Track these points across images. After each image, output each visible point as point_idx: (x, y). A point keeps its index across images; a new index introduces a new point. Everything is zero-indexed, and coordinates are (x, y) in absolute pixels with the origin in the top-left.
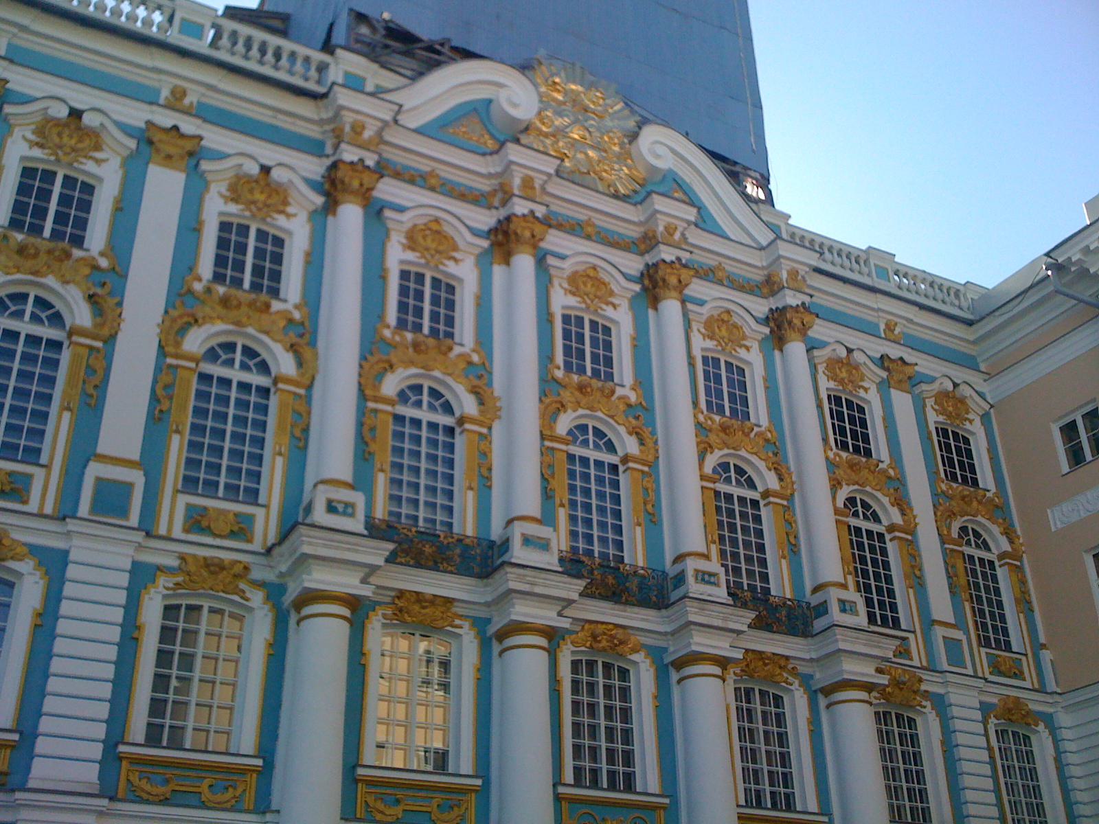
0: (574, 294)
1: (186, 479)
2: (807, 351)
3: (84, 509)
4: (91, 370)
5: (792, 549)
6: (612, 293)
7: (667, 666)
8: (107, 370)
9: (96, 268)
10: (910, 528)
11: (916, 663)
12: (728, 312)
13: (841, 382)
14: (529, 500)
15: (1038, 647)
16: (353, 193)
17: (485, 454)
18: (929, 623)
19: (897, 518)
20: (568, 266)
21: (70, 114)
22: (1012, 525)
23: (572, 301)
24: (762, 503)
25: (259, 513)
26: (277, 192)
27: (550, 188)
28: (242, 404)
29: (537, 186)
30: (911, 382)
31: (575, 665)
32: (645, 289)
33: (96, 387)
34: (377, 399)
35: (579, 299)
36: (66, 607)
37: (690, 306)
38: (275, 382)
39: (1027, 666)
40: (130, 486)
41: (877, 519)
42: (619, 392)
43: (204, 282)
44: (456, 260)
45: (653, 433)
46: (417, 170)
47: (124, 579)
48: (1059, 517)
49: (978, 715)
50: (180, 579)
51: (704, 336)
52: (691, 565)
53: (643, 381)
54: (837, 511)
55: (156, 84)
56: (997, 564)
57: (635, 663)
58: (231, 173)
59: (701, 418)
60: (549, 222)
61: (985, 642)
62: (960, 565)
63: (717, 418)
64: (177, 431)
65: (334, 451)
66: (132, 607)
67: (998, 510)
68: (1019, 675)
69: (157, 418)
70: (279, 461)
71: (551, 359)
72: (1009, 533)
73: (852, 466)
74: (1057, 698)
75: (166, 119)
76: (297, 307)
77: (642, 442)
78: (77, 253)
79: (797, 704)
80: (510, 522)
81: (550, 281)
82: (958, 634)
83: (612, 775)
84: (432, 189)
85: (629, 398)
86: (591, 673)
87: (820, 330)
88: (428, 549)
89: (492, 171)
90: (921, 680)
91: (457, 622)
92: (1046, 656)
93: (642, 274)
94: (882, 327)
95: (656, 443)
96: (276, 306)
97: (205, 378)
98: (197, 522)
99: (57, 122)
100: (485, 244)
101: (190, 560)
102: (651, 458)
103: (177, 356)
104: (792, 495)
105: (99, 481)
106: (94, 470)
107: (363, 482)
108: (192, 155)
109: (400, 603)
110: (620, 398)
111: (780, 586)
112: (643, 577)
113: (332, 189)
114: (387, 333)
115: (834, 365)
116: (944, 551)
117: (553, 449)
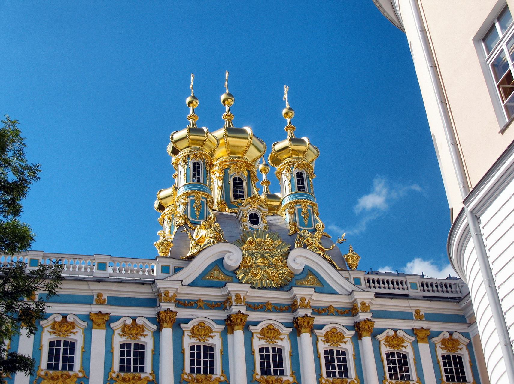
0: (263, 339)
9: (78, 378)
12: (334, 328)
20: (259, 327)
27: (248, 294)
29: (242, 297)
35: (265, 340)
37: (316, 331)
44: (212, 337)
51: (324, 342)
55: (91, 294)
71: (254, 371)
75: (96, 309)
76: (151, 374)
78: (71, 373)
81: (252, 336)
85: (289, 381)
89: (224, 293)
93: (293, 322)
94: (414, 313)
96: (143, 375)
100: (223, 327)
108: (108, 321)
113: (159, 321)
114: (186, 377)
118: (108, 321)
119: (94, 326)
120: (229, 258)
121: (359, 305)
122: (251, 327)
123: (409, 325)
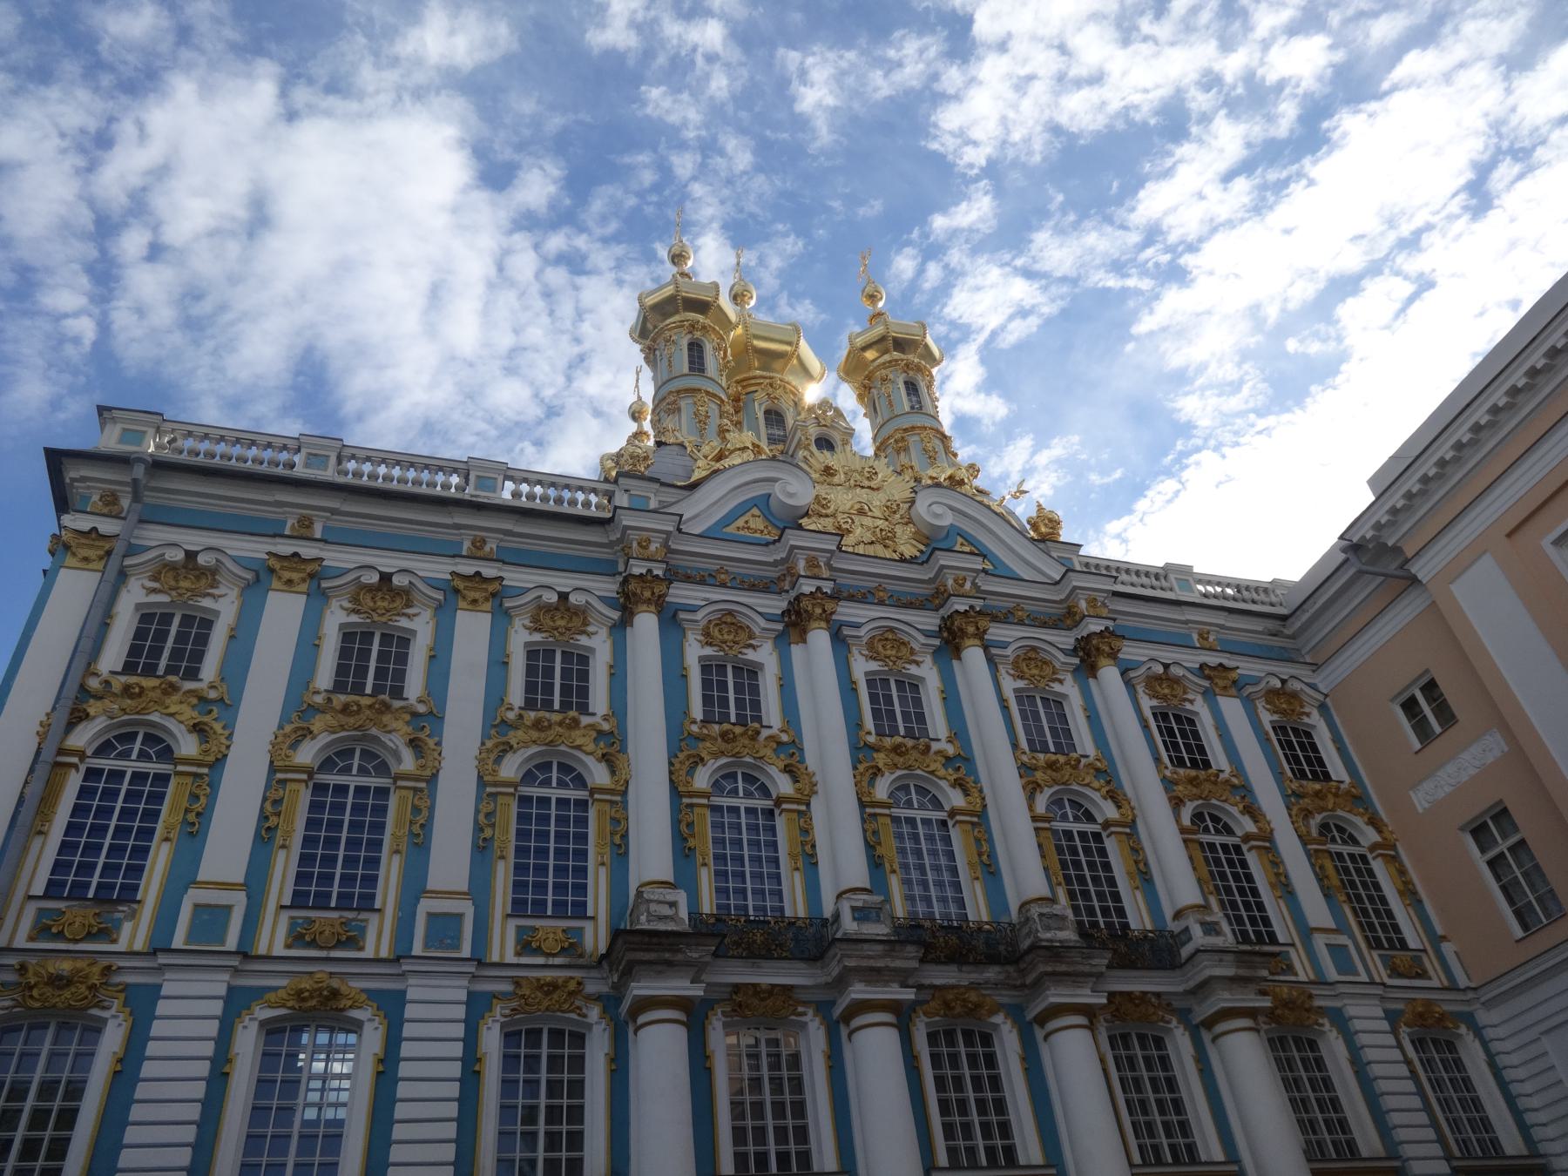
0: (874, 659)
1: (515, 902)
2: (1122, 674)
3: (417, 949)
4: (416, 810)
5: (1143, 876)
6: (912, 651)
7: (1030, 1023)
8: (432, 809)
9: (415, 715)
11: (1302, 977)
13: (1164, 698)
14: (856, 871)
15: (1437, 940)
16: (648, 602)
17: (806, 831)
18: (1307, 932)
19: (1249, 826)
21: (381, 579)
22: (1376, 812)
24: (1104, 835)
25: (588, 926)
26: (576, 614)
28: (563, 821)
30: (1237, 686)
31: (932, 1038)
32: (946, 642)
33: (422, 826)
34: (691, 795)
37: (994, 651)
38: (591, 795)
39: (1430, 964)
40: (459, 917)
41: (1230, 832)
42: (935, 746)
43: (517, 710)
45: (977, 781)
46: (705, 570)
47: (460, 1011)
48: (1421, 799)
49: (1385, 1025)
50: (514, 1004)
52: (1035, 911)
53: (958, 732)
54: (1183, 830)
55: (457, 538)
56: (1370, 857)
57: (996, 1026)
58: (531, 607)
59: (1025, 758)
60: (836, 596)
61: (1375, 944)
62: (1328, 864)
63: (1041, 756)
64: (502, 857)
65: (652, 855)
66: (471, 1040)
67: (1358, 799)
68: (1423, 975)
69: (482, 848)
70: (603, 871)
71: (860, 726)
72: (1374, 822)
73: (1192, 781)
74: (1470, 995)
75: (468, 568)
76: (605, 718)
77: (966, 793)
78: (397, 704)
79: (1180, 1045)
80: (839, 896)
82: (1343, 940)
83: (990, 1151)
84: (723, 585)
86: (951, 1042)
87: (1130, 651)
88: (759, 938)
90: (1311, 996)
91: (800, 1009)
92: (1448, 949)
94: (1195, 637)
95: (981, 791)
97: (525, 801)
98: (526, 945)
99: (370, 588)
101: (524, 982)
102: (978, 808)
103: (495, 784)
104: (1134, 821)
105: (432, 916)
106: (425, 906)
107: (684, 878)
108: (495, 597)
109: (738, 998)
110: (939, 752)
111: (1138, 918)
112: (989, 931)
113: (627, 606)
114: (695, 728)
115: (1153, 682)
116: (1308, 854)
117: (875, 815)
119: (462, 604)
121: (1083, 605)
123: (1193, 659)
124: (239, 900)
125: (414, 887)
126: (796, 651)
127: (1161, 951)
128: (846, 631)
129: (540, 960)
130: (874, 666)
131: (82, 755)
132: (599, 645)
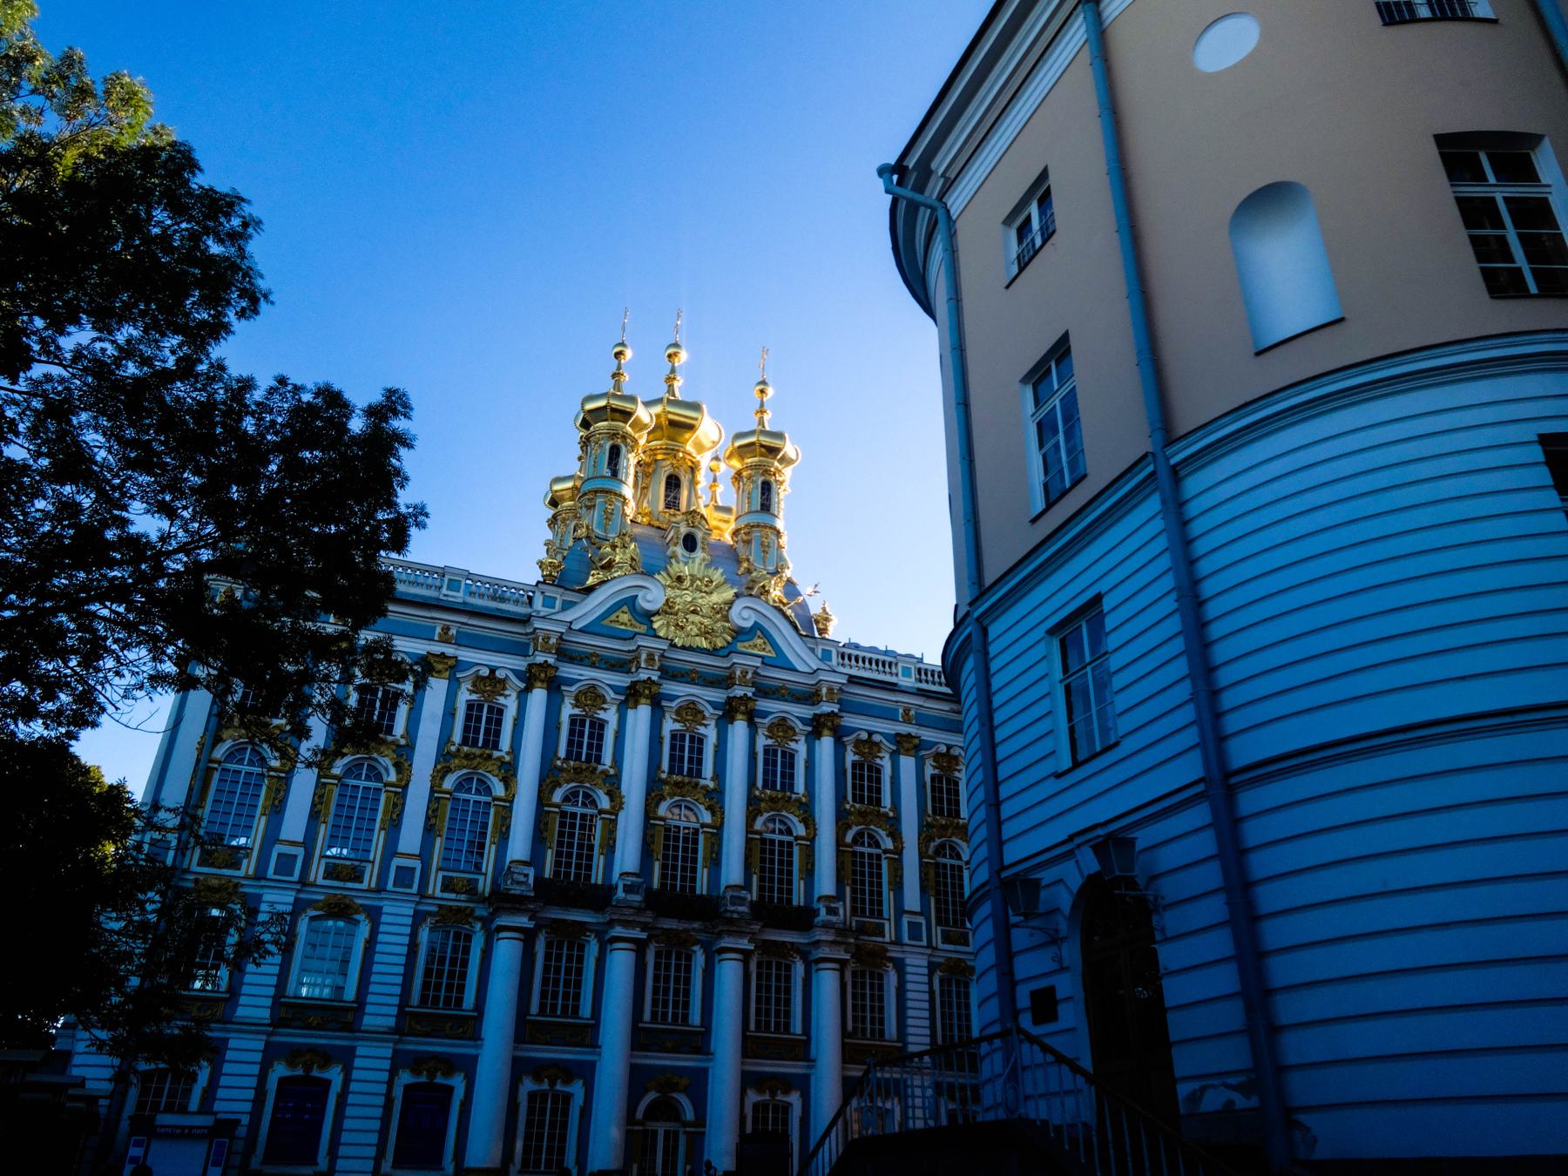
3: (390, 886)
4: (395, 805)
6: (704, 718)
8: (404, 804)
9: (399, 746)
10: (899, 850)
11: (887, 939)
18: (900, 911)
23: (678, 726)
25: (481, 878)
36: (381, 937)
47: (409, 921)
49: (925, 971)
66: (413, 935)
71: (659, 766)
75: (437, 648)
77: (713, 814)
78: (390, 738)
96: (496, 754)
98: (448, 885)
105: (399, 868)
107: (536, 859)
116: (921, 864)
118: (453, 667)
120: (644, 598)
121: (824, 691)
122: (664, 703)
124: (300, 852)
125: (391, 851)
126: (630, 712)
127: (803, 918)
128: (664, 703)
129: (453, 896)
130: (678, 726)
131: (219, 762)
132: (510, 703)
